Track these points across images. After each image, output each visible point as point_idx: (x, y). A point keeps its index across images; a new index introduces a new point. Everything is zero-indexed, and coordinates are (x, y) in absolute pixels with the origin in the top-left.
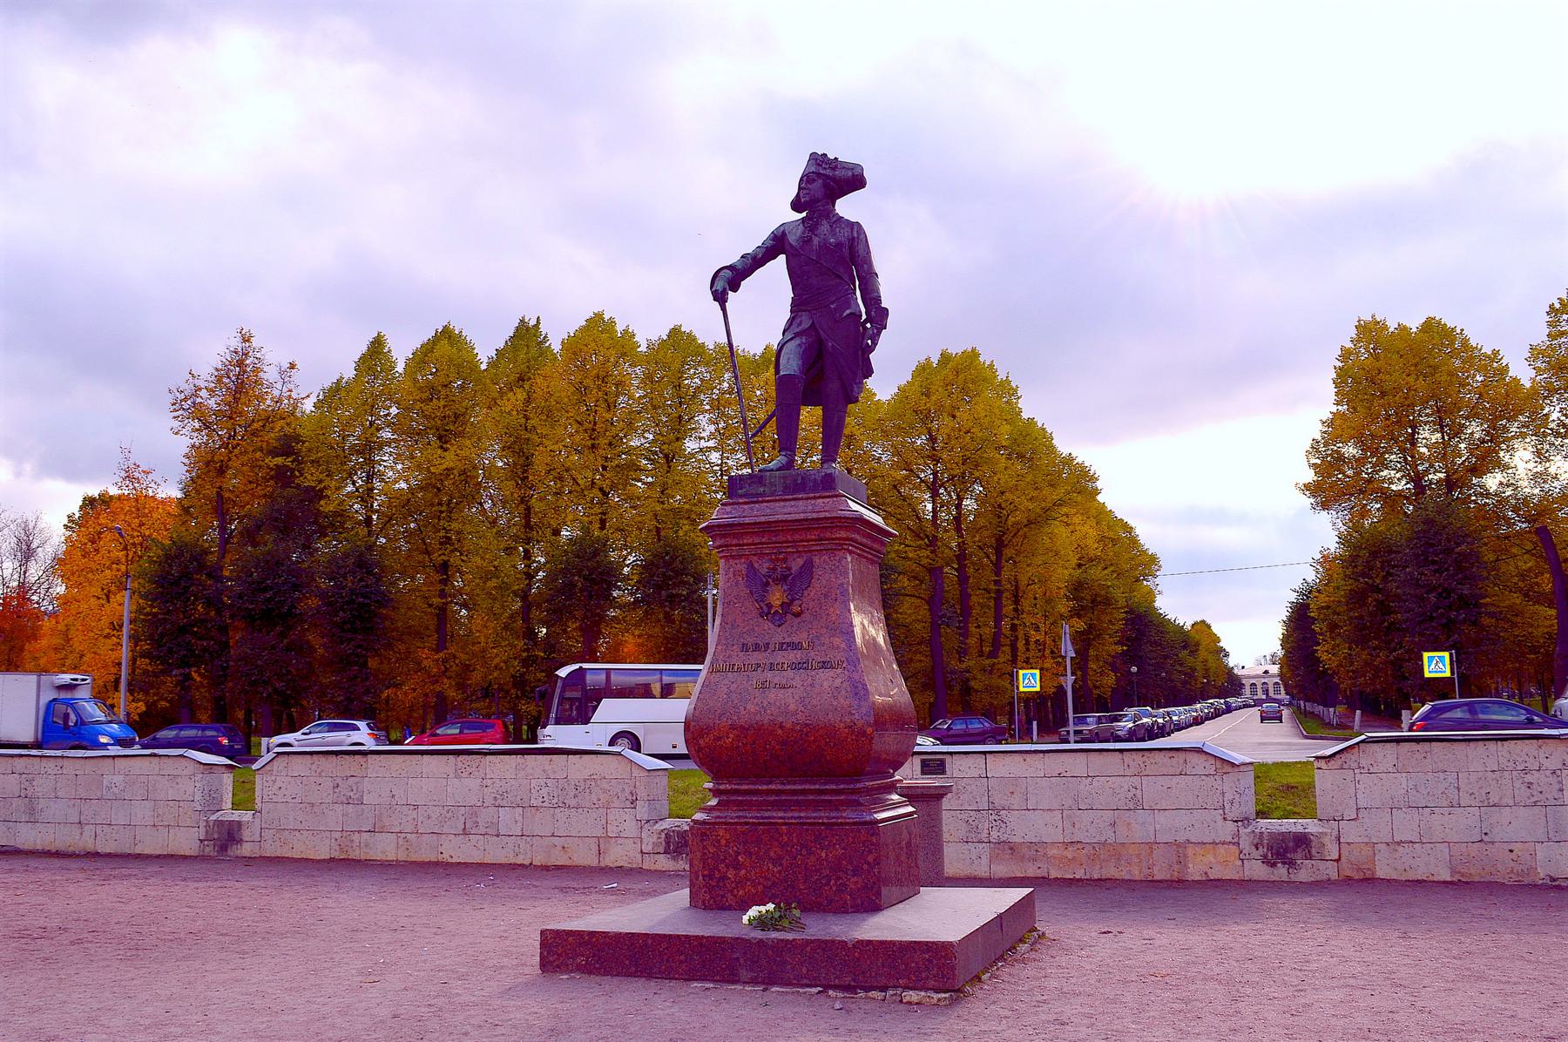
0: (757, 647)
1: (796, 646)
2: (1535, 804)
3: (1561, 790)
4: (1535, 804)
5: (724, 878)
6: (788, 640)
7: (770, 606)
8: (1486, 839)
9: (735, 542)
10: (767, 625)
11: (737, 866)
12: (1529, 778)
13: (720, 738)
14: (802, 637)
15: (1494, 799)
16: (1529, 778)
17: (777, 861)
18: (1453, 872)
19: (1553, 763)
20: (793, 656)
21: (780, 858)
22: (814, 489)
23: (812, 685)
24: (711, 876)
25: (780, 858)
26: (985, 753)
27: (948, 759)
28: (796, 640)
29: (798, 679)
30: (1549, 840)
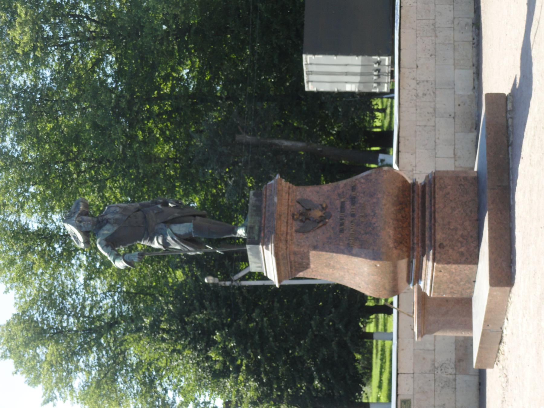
0: (342, 224)
1: (343, 204)
2: (434, 93)
3: (427, 81)
4: (434, 93)
5: (462, 236)
6: (339, 210)
7: (321, 217)
8: (453, 115)
9: (285, 235)
10: (330, 221)
11: (456, 229)
12: (420, 94)
13: (390, 236)
14: (338, 203)
15: (431, 110)
16: (420, 94)
17: (453, 209)
18: (471, 131)
19: (413, 84)
20: (348, 205)
21: (451, 207)
22: (261, 201)
23: (364, 193)
24: (461, 243)
25: (451, 207)
26: (398, 374)
27: (400, 398)
28: (339, 206)
29: (361, 200)
30: (454, 88)
